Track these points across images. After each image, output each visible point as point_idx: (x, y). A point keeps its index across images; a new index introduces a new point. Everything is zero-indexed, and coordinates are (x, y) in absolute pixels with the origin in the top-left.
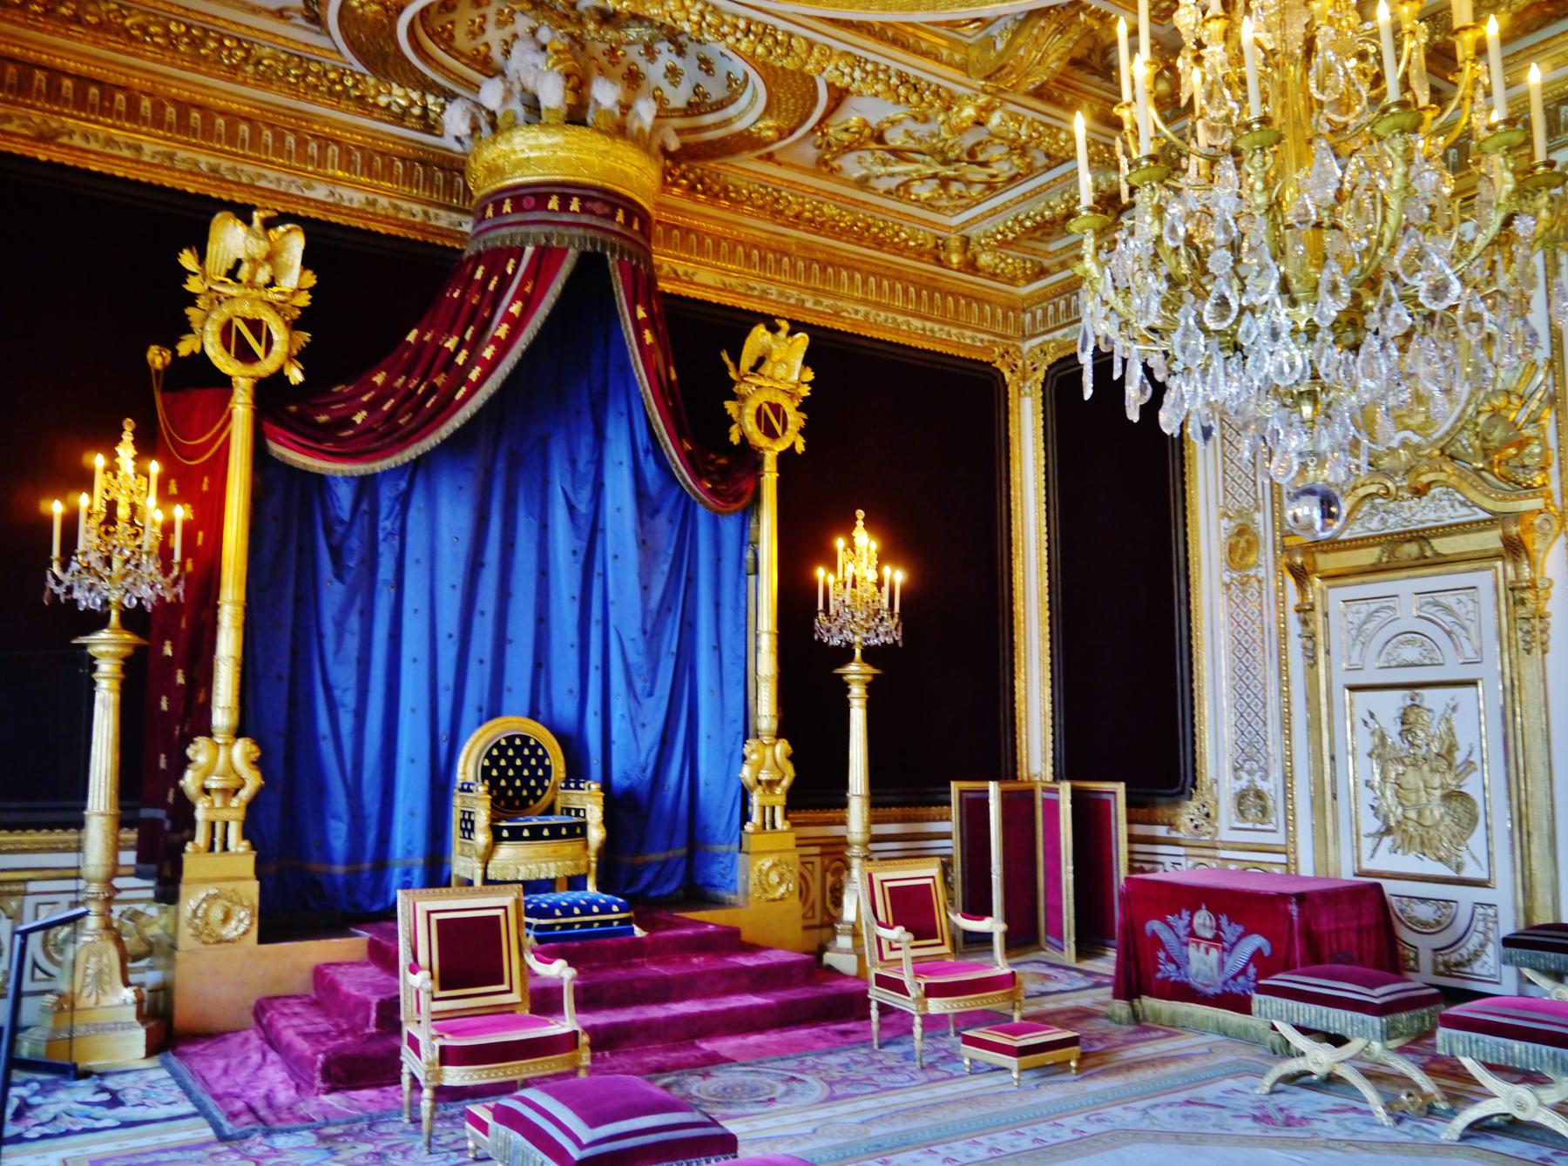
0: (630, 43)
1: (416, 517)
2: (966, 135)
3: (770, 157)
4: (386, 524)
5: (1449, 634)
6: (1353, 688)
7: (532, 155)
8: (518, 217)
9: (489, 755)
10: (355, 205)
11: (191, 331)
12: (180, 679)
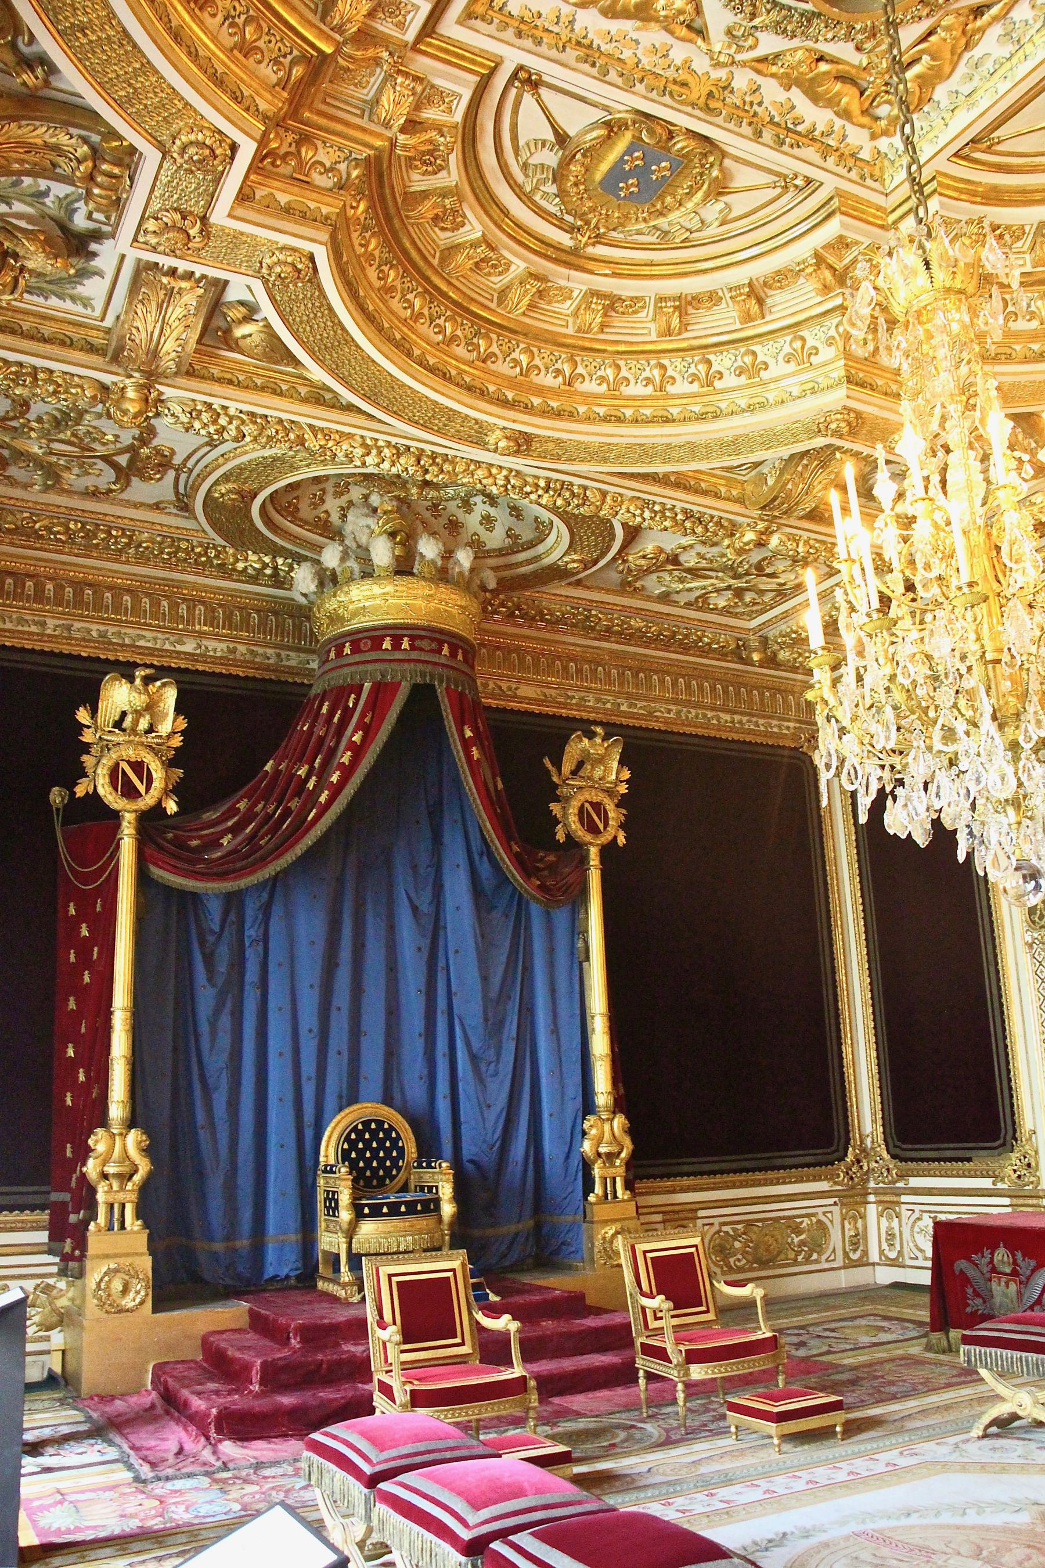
1: (276, 925)
2: (752, 553)
3: (578, 583)
4: (251, 932)
8: (357, 658)
9: (347, 1139)
10: (218, 654)
11: (85, 775)
12: (82, 1077)
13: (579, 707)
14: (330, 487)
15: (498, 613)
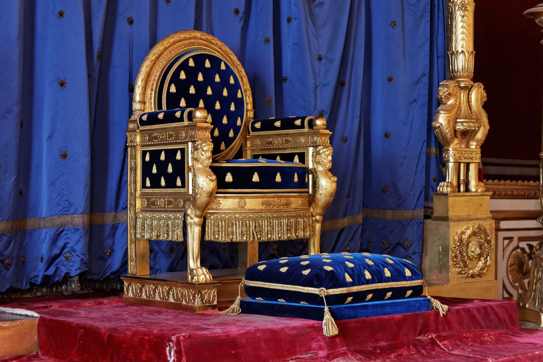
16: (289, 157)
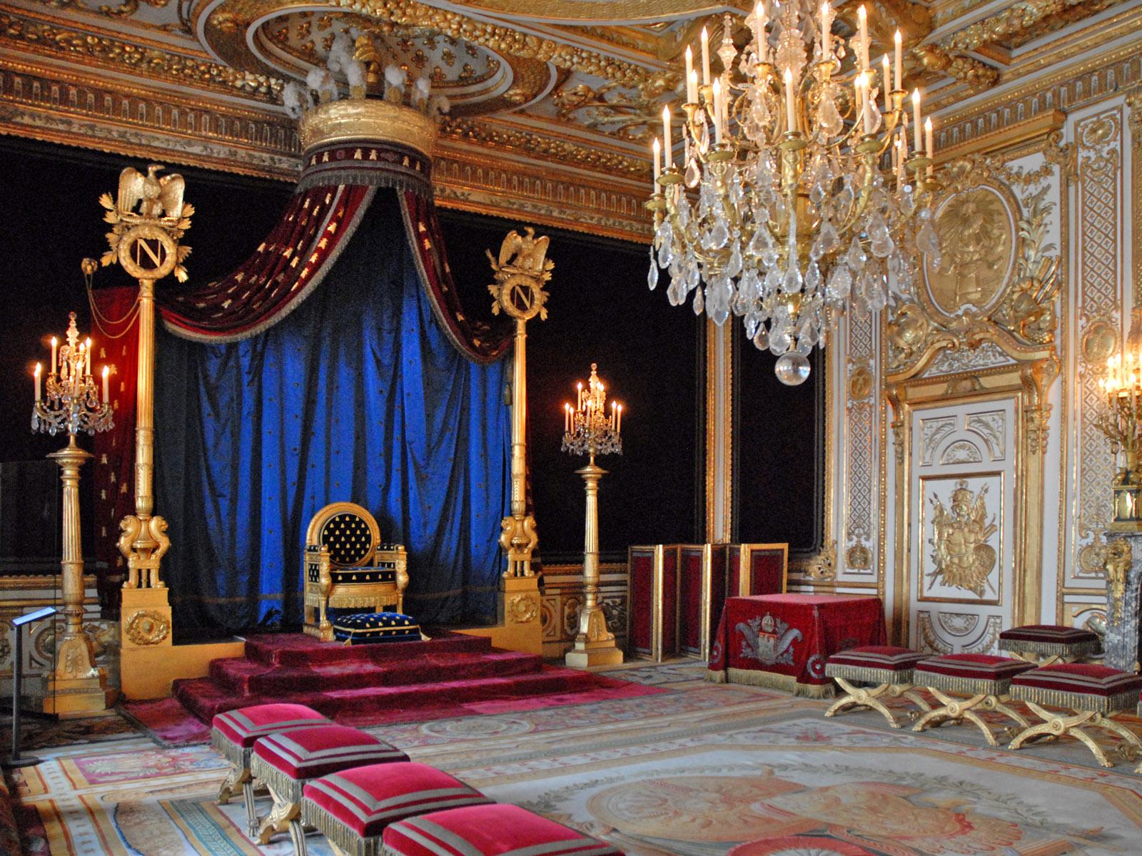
0: (415, 37)
3: (522, 112)
5: (986, 441)
6: (925, 478)
7: (343, 121)
8: (333, 165)
12: (113, 479)
13: (520, 210)
14: (314, 20)
15: (456, 133)
16: (389, 565)
